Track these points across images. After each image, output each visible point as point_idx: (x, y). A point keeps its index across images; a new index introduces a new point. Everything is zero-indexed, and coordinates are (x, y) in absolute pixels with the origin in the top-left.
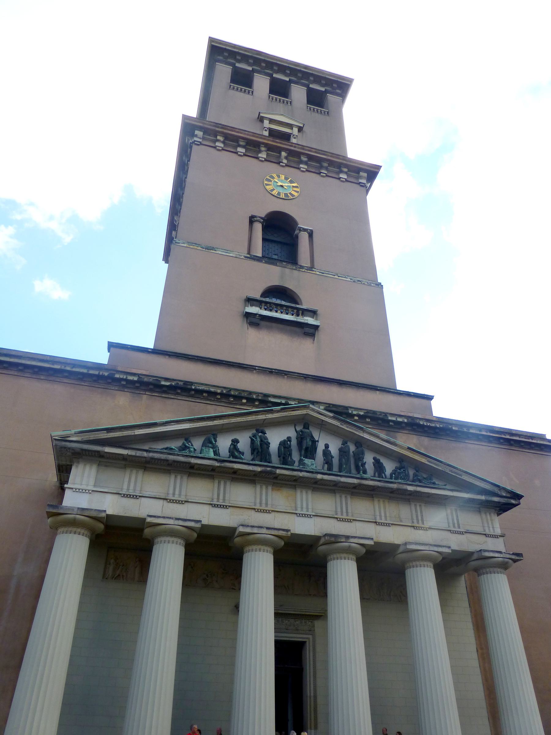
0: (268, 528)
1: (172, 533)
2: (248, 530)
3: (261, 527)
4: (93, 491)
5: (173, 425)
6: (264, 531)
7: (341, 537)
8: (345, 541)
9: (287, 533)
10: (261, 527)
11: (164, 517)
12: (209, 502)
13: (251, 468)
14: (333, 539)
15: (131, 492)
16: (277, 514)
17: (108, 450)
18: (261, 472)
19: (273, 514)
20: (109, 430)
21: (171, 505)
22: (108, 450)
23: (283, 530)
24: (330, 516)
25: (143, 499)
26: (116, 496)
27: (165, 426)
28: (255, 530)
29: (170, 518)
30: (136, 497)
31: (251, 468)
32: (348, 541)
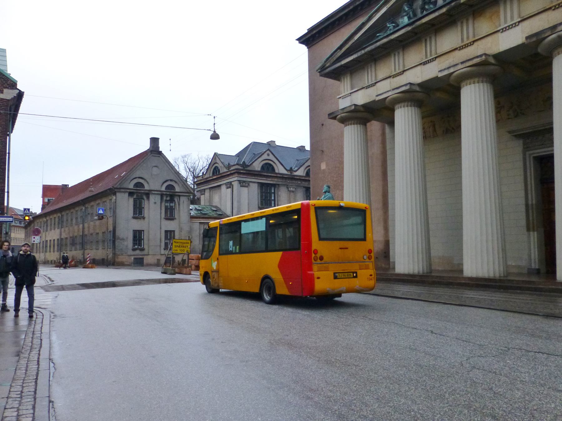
0: (462, 63)
1: (397, 101)
2: (446, 73)
3: (456, 65)
4: (351, 93)
5: (375, 16)
6: (460, 66)
7: (545, 31)
8: (550, 34)
9: (481, 58)
10: (456, 65)
11: (385, 92)
12: (419, 63)
13: (437, 14)
14: (534, 39)
15: (370, 83)
16: (479, 43)
17: (344, 62)
18: (447, 11)
19: (476, 44)
20: (340, 48)
21: (395, 79)
22: (344, 62)
23: (477, 57)
24: (540, 11)
25: (378, 84)
26: (363, 90)
27: (370, 20)
28: (452, 70)
29: (388, 91)
30: (374, 85)
31: (437, 14)
32: (556, 31)
